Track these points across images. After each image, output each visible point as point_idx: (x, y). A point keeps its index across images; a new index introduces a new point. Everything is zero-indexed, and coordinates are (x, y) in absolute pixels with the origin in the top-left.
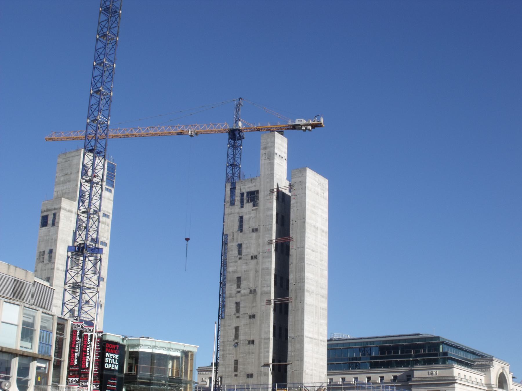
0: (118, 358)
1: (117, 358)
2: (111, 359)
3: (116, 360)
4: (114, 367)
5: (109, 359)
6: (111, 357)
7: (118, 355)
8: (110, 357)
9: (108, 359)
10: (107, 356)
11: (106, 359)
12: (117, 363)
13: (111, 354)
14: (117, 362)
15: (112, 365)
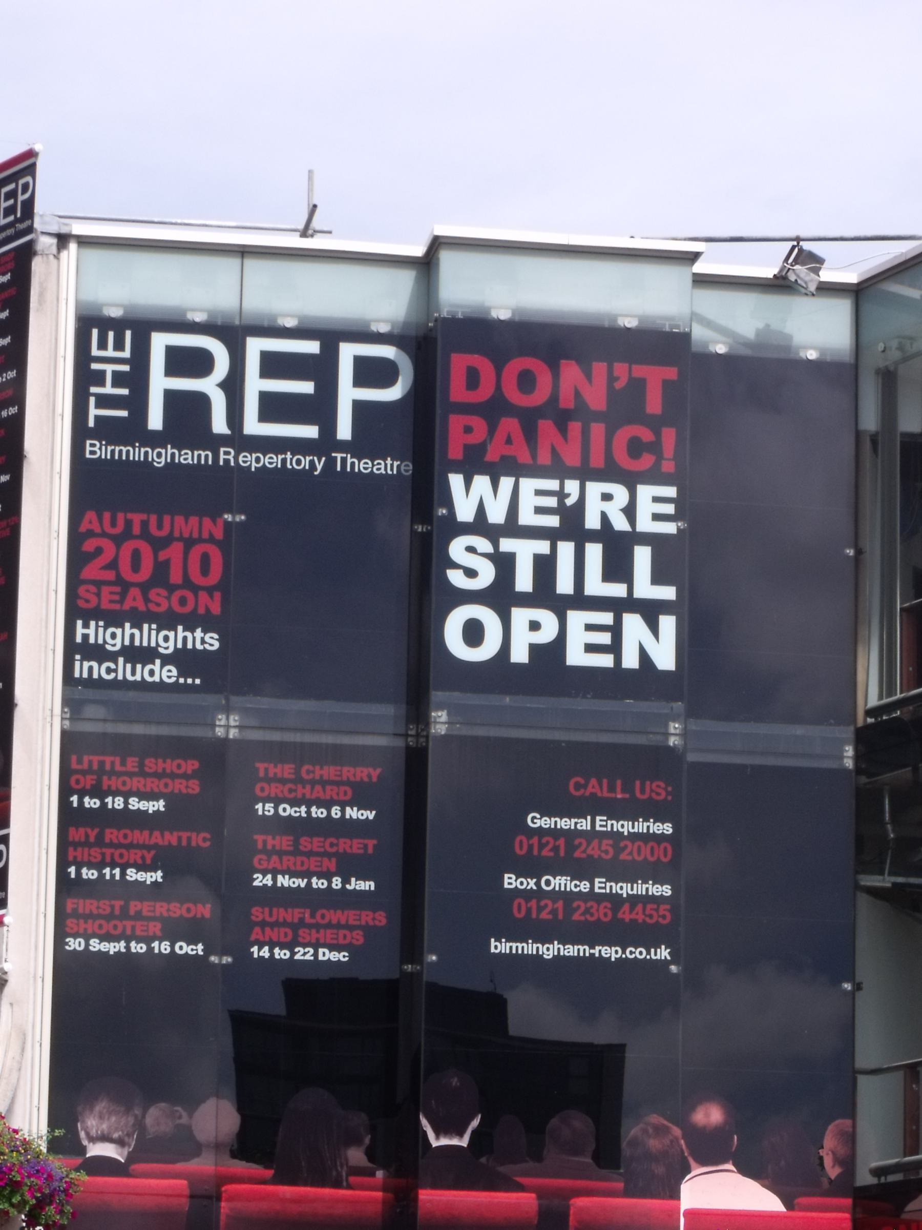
0: (670, 528)
1: (645, 524)
2: (543, 547)
3: (642, 557)
4: (605, 638)
5: (507, 545)
6: (553, 521)
7: (671, 492)
8: (527, 517)
9: (484, 545)
10: (465, 512)
11: (457, 549)
12: (668, 593)
13: (553, 485)
14: (658, 578)
15: (577, 619)
